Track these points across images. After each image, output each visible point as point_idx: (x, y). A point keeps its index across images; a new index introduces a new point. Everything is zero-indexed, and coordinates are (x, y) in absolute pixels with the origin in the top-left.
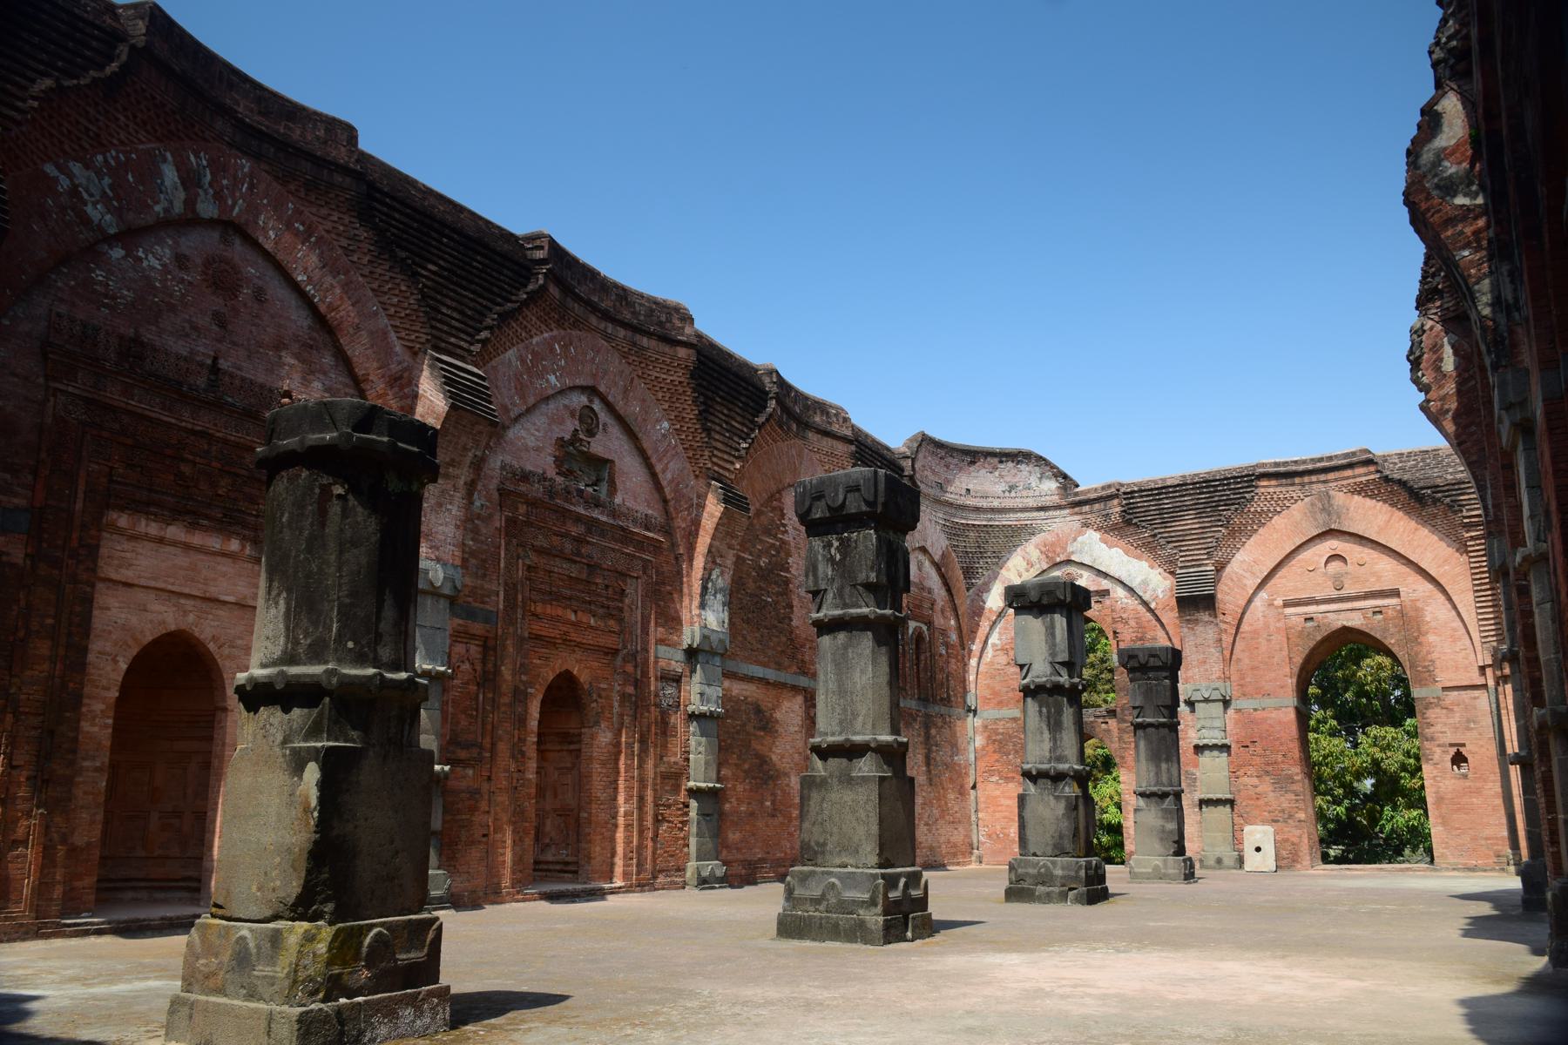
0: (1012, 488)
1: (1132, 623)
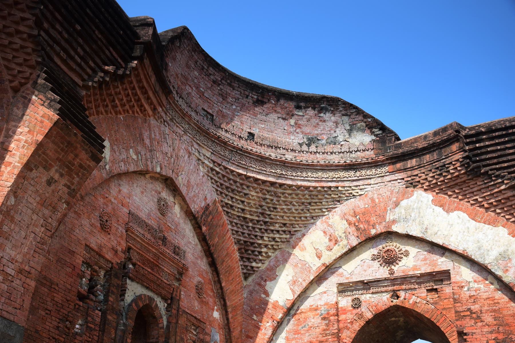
1: (488, 318)
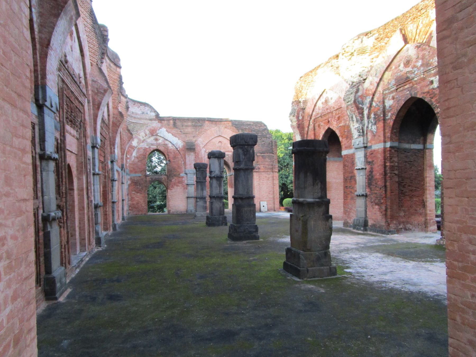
0: (143, 113)
